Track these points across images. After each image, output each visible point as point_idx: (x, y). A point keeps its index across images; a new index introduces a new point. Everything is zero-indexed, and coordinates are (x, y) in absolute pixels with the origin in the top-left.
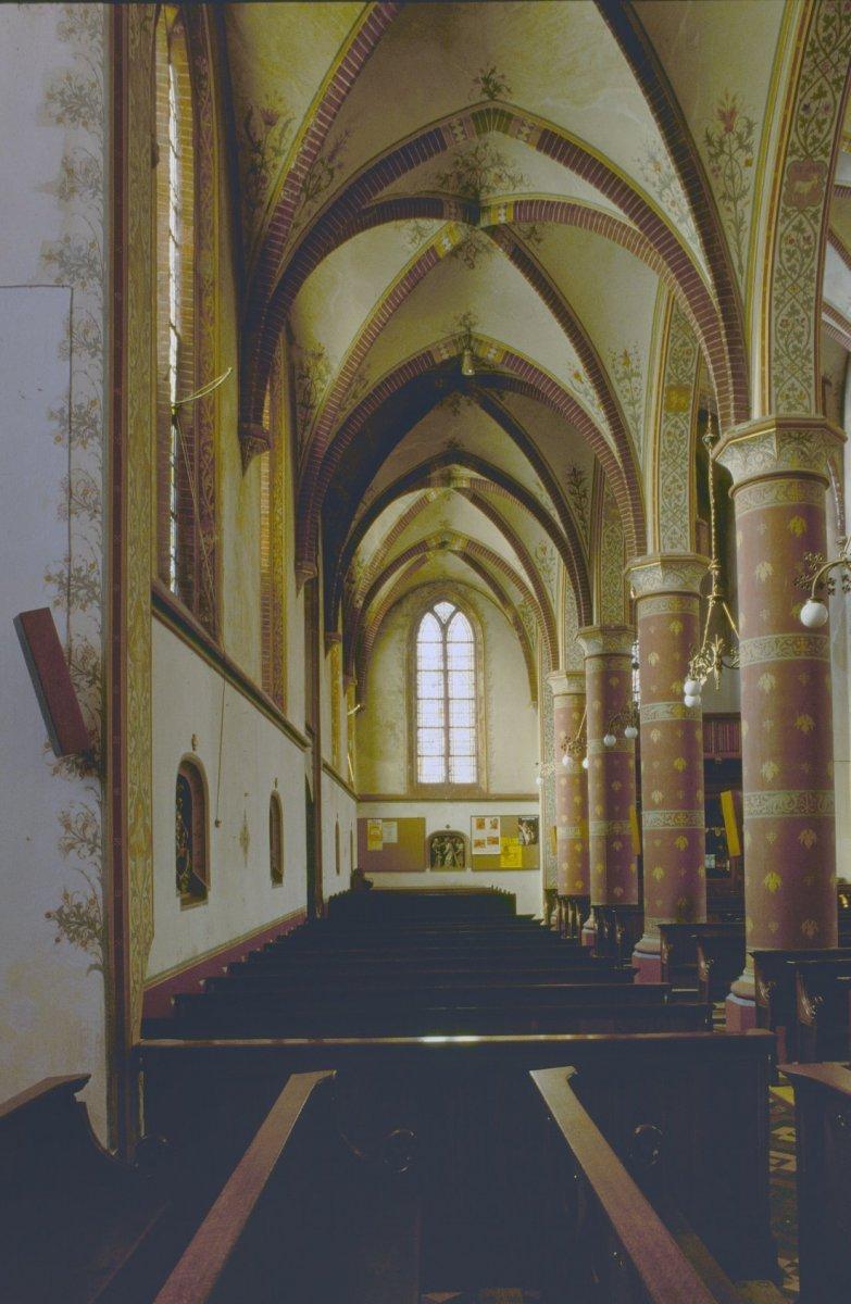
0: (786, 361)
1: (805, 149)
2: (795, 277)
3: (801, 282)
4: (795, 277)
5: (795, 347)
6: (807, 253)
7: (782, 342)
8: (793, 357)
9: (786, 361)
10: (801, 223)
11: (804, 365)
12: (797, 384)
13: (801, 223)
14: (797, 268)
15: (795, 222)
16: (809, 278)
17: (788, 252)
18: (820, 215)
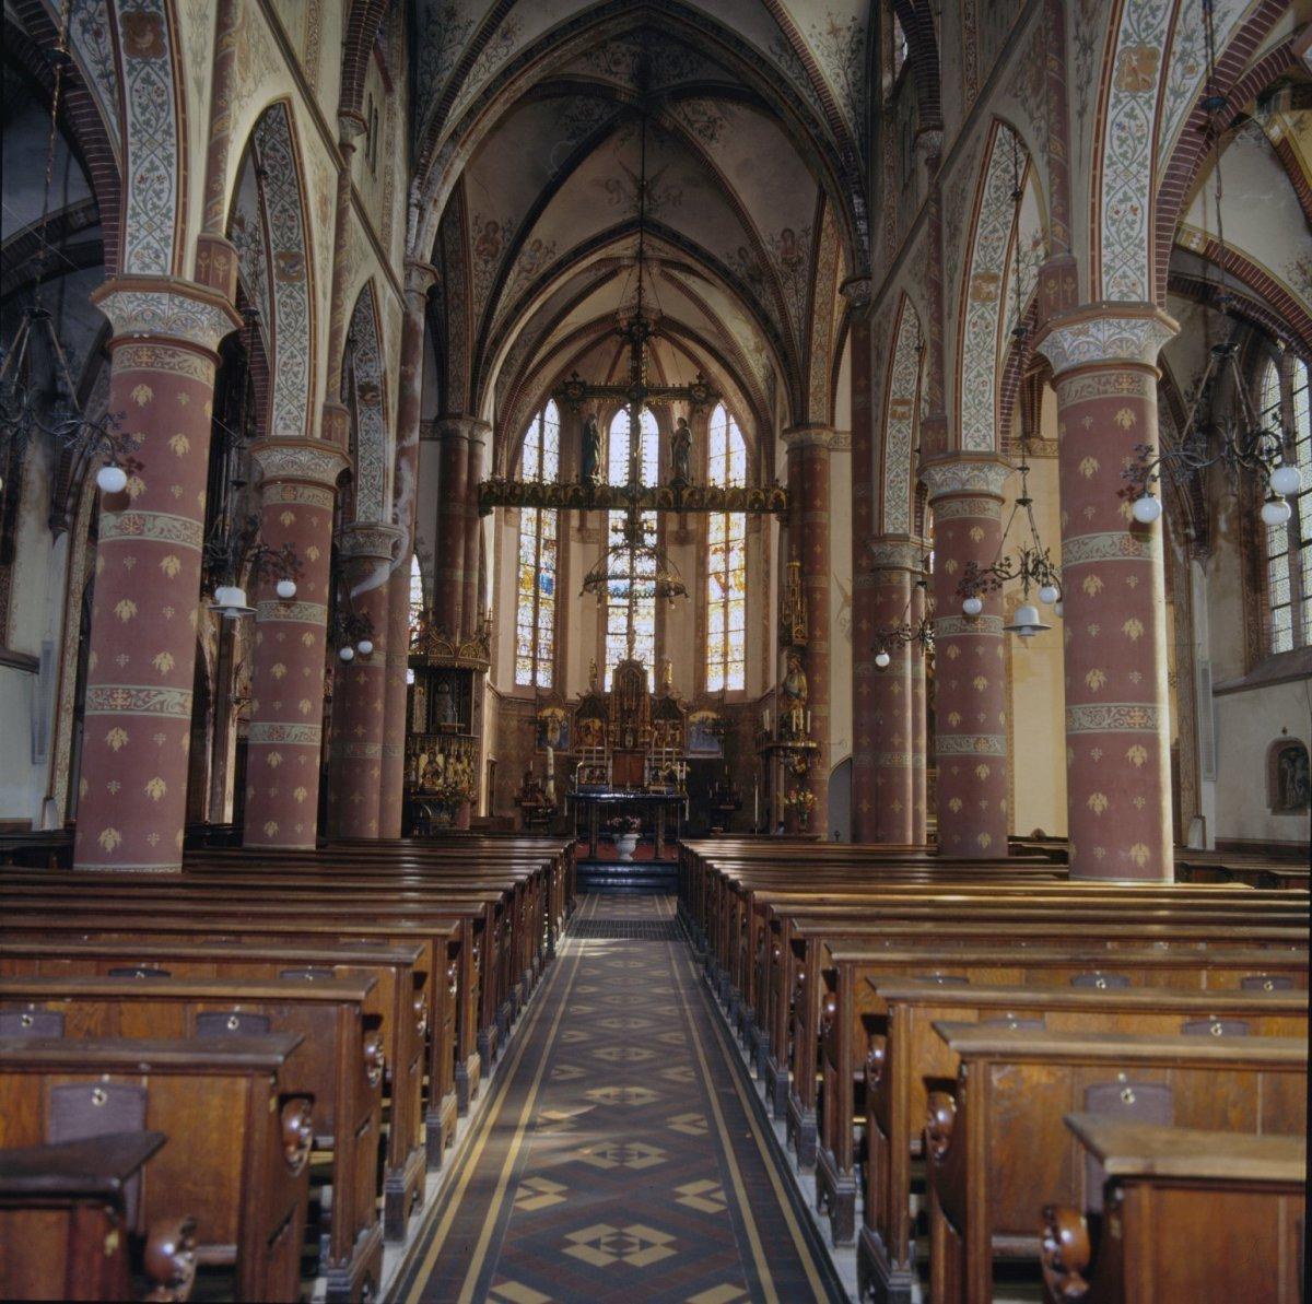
0: (1117, 248)
1: (1139, 36)
2: (1127, 163)
3: (1134, 168)
4: (1127, 163)
5: (1127, 235)
6: (1139, 140)
7: (1113, 229)
8: (1126, 244)
9: (1117, 248)
10: (1133, 109)
11: (1136, 254)
12: (1129, 273)
13: (1133, 109)
14: (1130, 155)
15: (1127, 109)
16: (1142, 165)
17: (1119, 138)
18: (1154, 102)
